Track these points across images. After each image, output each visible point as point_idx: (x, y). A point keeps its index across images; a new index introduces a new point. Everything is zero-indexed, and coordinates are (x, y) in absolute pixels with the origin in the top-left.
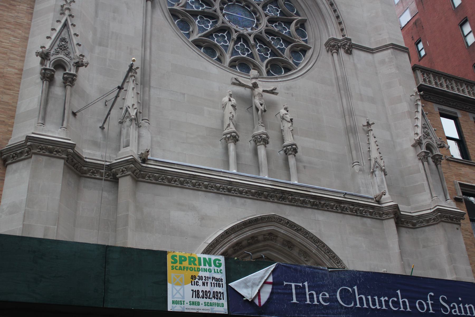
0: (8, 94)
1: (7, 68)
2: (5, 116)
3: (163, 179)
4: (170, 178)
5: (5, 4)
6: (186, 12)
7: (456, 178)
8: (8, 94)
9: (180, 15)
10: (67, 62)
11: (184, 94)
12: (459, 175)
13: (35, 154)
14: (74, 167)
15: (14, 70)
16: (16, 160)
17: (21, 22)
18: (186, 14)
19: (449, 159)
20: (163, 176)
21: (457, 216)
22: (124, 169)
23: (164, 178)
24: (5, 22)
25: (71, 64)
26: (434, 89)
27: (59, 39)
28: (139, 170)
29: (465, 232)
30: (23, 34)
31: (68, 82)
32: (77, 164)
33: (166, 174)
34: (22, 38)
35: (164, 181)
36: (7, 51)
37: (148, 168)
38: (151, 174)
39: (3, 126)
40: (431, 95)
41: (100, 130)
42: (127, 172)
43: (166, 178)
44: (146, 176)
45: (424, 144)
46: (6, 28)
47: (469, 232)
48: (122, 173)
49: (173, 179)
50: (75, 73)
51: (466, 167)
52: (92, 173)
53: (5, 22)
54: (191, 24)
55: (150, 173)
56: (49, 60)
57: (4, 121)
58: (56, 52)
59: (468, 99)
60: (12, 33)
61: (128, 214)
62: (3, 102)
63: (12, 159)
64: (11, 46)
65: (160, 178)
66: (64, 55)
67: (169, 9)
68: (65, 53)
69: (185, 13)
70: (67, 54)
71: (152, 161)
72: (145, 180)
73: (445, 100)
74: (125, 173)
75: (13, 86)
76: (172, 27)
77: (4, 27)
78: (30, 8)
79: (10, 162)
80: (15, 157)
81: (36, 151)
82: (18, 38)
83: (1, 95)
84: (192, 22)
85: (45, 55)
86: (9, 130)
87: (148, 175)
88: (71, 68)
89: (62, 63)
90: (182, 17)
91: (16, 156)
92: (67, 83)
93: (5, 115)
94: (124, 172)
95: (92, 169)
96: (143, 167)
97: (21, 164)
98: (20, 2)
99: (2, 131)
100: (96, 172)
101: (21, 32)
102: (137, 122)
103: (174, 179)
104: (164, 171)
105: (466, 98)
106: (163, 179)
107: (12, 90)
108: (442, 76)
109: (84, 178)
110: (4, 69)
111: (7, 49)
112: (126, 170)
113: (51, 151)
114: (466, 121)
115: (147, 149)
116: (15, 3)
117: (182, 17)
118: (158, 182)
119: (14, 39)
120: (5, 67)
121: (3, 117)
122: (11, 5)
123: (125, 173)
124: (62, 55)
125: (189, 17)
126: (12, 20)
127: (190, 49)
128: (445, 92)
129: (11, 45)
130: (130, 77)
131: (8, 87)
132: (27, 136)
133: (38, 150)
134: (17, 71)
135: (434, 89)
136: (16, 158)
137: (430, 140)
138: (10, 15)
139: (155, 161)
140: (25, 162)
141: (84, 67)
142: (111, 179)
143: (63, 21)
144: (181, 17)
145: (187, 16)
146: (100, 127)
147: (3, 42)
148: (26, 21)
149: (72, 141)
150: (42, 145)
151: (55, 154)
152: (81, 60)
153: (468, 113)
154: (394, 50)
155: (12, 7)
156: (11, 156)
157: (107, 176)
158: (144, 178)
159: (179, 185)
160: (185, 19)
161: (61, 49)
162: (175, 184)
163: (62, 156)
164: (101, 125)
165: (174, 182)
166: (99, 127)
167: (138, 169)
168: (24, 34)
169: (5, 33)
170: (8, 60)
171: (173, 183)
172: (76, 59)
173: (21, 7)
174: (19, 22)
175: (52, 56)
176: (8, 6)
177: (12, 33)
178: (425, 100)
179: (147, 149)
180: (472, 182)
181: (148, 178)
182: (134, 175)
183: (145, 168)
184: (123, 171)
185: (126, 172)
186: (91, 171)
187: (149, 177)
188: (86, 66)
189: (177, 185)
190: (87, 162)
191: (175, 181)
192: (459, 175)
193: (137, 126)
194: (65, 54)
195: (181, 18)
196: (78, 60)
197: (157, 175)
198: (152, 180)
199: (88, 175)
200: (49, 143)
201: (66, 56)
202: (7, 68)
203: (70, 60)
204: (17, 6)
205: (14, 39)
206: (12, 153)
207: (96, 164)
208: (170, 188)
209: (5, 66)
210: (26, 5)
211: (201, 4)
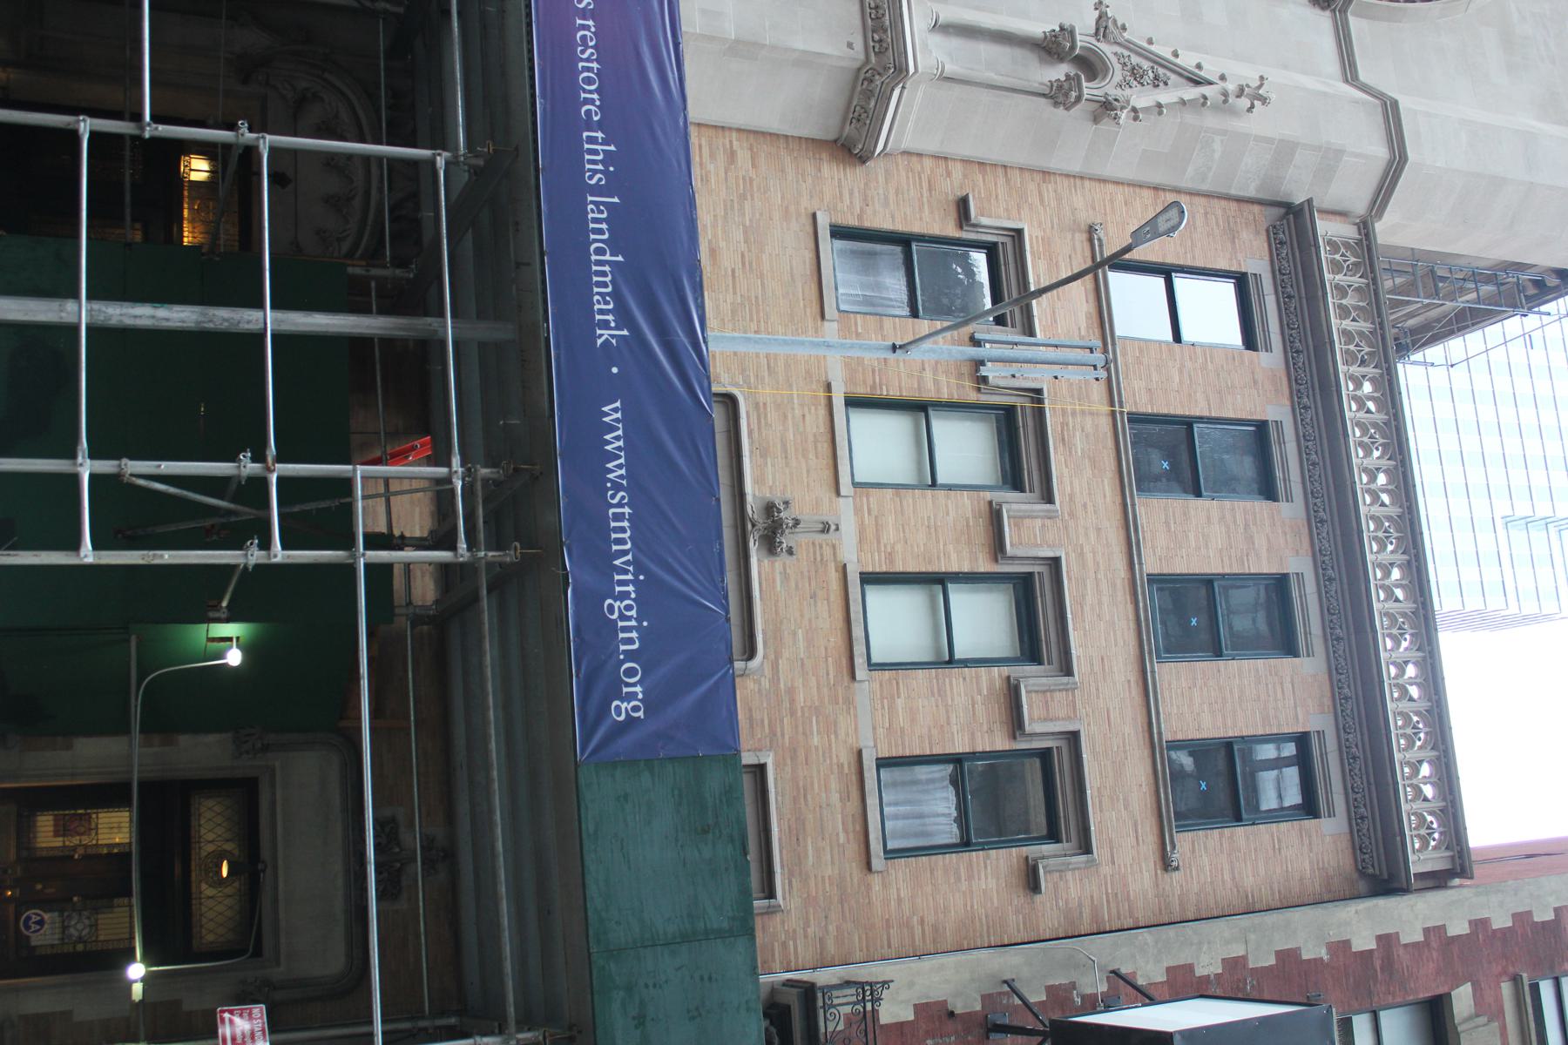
7: (1037, 237)
12: (1051, 259)
19: (1095, 236)
21: (889, 40)
26: (1313, 249)
29: (859, 191)
40: (1341, 583)
45: (1098, 44)
47: (861, 209)
51: (1087, 302)
59: (1334, 389)
73: (1298, 306)
105: (1334, 384)
108: (1391, 415)
114: (1255, 382)
128: (1320, 293)
135: (1313, 249)
137: (1118, 77)
153: (1287, 402)
154: (1380, 109)
178: (1267, 231)
180: (1044, 306)
192: (1051, 259)
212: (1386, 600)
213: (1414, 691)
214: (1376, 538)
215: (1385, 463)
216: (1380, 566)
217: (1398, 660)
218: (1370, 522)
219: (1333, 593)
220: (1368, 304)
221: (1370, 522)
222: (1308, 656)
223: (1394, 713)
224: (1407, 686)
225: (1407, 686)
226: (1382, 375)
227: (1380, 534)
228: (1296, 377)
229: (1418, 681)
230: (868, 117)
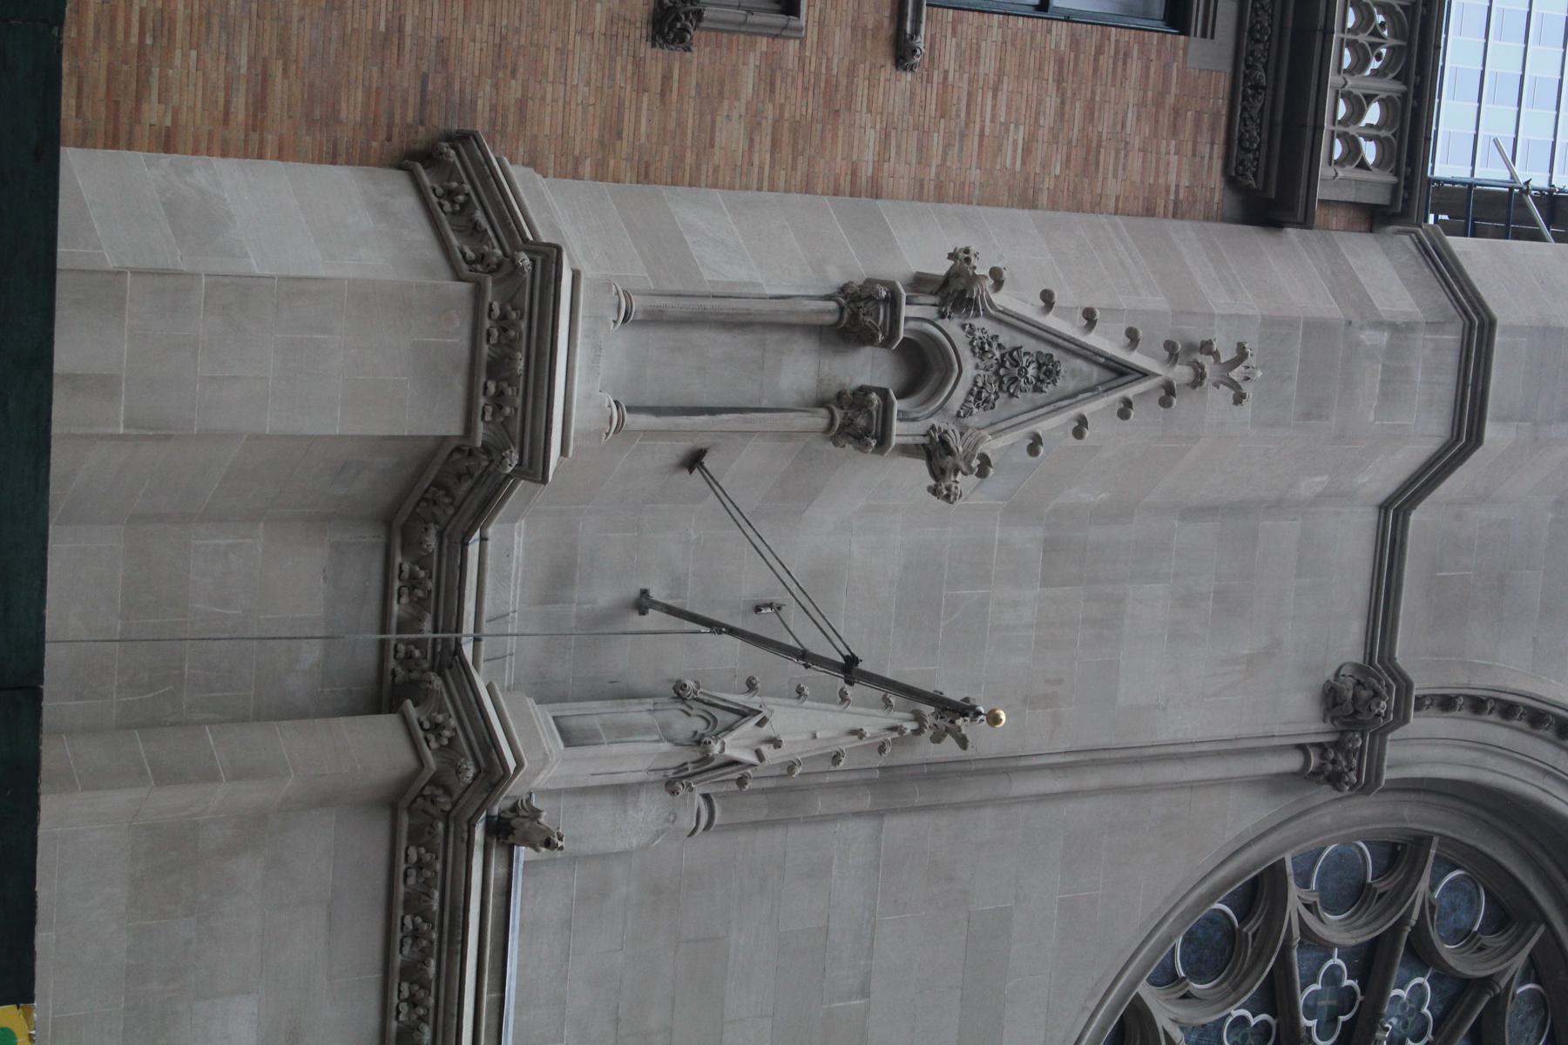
0: (751, 141)
1: (878, 127)
2: (643, 139)
3: (416, 935)
4: (426, 972)
5: (1174, 90)
6: (1278, 949)
8: (751, 141)
9: (1259, 922)
10: (941, 400)
11: (864, 993)
13: (478, 293)
14: (433, 489)
15: (869, 156)
16: (439, 209)
17: (1101, 169)
18: (1273, 953)
20: (435, 936)
22: (447, 733)
23: (425, 943)
24: (1093, 93)
25: (934, 421)
27: (1046, 349)
28: (448, 808)
30: (1048, 183)
31: (846, 414)
32: (447, 500)
33: (445, 946)
34: (1027, 180)
35: (409, 941)
36: (958, 116)
37: (465, 854)
38: (436, 873)
39: (596, 136)
41: (633, 592)
42: (434, 753)
43: (422, 950)
44: (423, 850)
46: (1063, 103)
48: (427, 725)
49: (425, 986)
50: (895, 440)
52: (413, 576)
53: (1093, 93)
54: (1225, 985)
55: (438, 866)
56: (942, 316)
57: (619, 135)
58: (983, 343)
60: (1043, 134)
61: (218, 780)
62: (713, 121)
63: (440, 191)
64: (982, 134)
65: (419, 920)
66: (975, 383)
67: (1283, 860)
68: (984, 384)
69: (1277, 942)
70: (980, 393)
71: (503, 871)
72: (404, 844)
74: (428, 742)
75: (795, 159)
76: (1194, 888)
77: (1069, 93)
78: (1176, 203)
79: (426, 180)
80: (453, 202)
81: (489, 298)
82: (1024, 163)
83: (743, 112)
84: (1235, 988)
85: (963, 292)
86: (577, 161)
87: (428, 857)
88: (914, 420)
89: (935, 378)
90: (1254, 935)
91: (457, 208)
92: (842, 408)
93: (648, 137)
94: (432, 737)
95: (430, 577)
96: (465, 827)
97: (419, 233)
98: (1194, 154)
99: (572, 134)
100: (419, 598)
101: (1058, 172)
102: (690, 771)
103: (422, 993)
104: (460, 938)
106: (416, 935)
107: (772, 154)
109: (382, 540)
110: (869, 111)
111: (963, 114)
112: (445, 742)
113: (498, 367)
115: (561, 839)
116: (1187, 132)
117: (1250, 934)
118: (400, 912)
119: (1015, 142)
120: (878, 117)
121: (636, 130)
122: (1176, 112)
123: (428, 742)
124: (976, 372)
125: (1261, 965)
126: (1104, 126)
127: (1099, 997)
129: (987, 131)
130: (912, 712)
131: (786, 137)
132: (559, 249)
133: (496, 305)
134: (870, 173)
136: (447, 206)
138: (1130, 115)
139: (505, 883)
140: (434, 254)
141: (933, 482)
142: (390, 677)
143: (1136, 359)
144: (1250, 929)
145: (1260, 956)
146: (644, 593)
147: (995, 97)
148: (1113, 187)
149: (559, 462)
150: (523, 325)
151: (486, 388)
152: (962, 465)
155: (1165, 118)
156: (455, 184)
157: (401, 655)
158: (415, 837)
159: (394, 1025)
160: (1247, 948)
161: (1001, 364)
162: (396, 1001)
163: (481, 425)
164: (656, 594)
165: (406, 994)
166: (643, 586)
167: (455, 805)
168: (1046, 185)
169: (1040, 102)
170: (916, 128)
171: (400, 992)
172: (964, 438)
173: (1174, 159)
174: (1102, 158)
175: (963, 327)
176: (1170, 100)
177: (1043, 134)
179: (561, 839)
181: (414, 857)
182: (423, 788)
183: (466, 837)
184: (436, 728)
185: (434, 745)
186: (422, 574)
187: (420, 865)
188: (934, 491)
189: (394, 1013)
190: (465, 545)
191: (413, 1002)
193: (670, 774)
194: (980, 384)
195: (1244, 930)
196: (961, 449)
197: (436, 906)
198: (405, 881)
199: (398, 559)
200: (539, 354)
201: (970, 393)
202: (878, 127)
203: (955, 413)
204: (1173, 142)
205: (1015, 142)
206: (467, 187)
207: (457, 592)
208: (375, 977)
209: (882, 113)
210: (1185, 182)
211: (1336, 1020)
212: (1340, 163)
213: (1370, 151)
214: (1352, 45)
215: (1390, 86)
216: (1348, 96)
217: (1356, 92)
218: (1341, 102)
219: (1255, 113)
220: (1394, 135)
221: (1341, 102)
222: (1204, 35)
223: (1337, 92)
224: (1362, 139)
225: (1362, 139)
226: (1404, 95)
227: (1363, 38)
228: (1241, 135)
229: (1383, 133)
230: (452, 504)
